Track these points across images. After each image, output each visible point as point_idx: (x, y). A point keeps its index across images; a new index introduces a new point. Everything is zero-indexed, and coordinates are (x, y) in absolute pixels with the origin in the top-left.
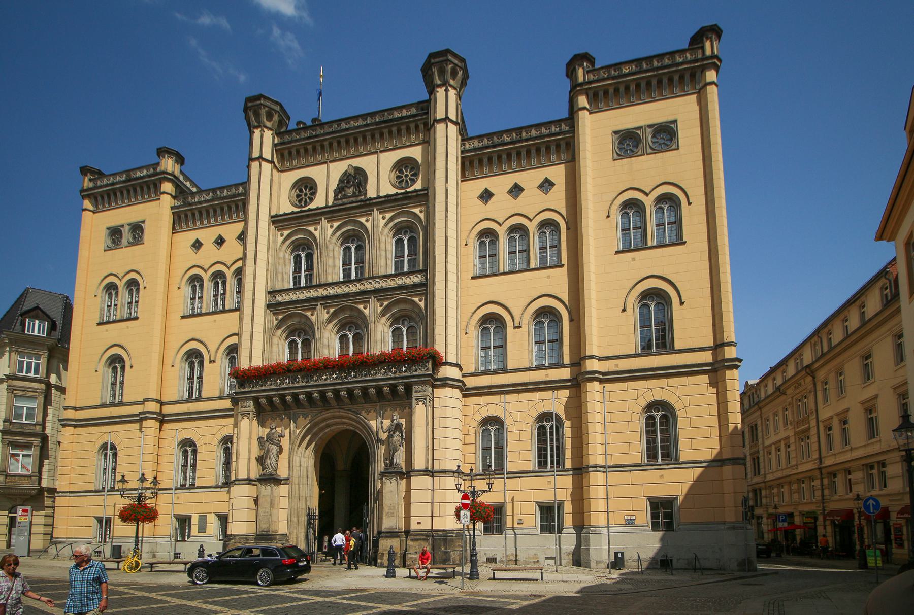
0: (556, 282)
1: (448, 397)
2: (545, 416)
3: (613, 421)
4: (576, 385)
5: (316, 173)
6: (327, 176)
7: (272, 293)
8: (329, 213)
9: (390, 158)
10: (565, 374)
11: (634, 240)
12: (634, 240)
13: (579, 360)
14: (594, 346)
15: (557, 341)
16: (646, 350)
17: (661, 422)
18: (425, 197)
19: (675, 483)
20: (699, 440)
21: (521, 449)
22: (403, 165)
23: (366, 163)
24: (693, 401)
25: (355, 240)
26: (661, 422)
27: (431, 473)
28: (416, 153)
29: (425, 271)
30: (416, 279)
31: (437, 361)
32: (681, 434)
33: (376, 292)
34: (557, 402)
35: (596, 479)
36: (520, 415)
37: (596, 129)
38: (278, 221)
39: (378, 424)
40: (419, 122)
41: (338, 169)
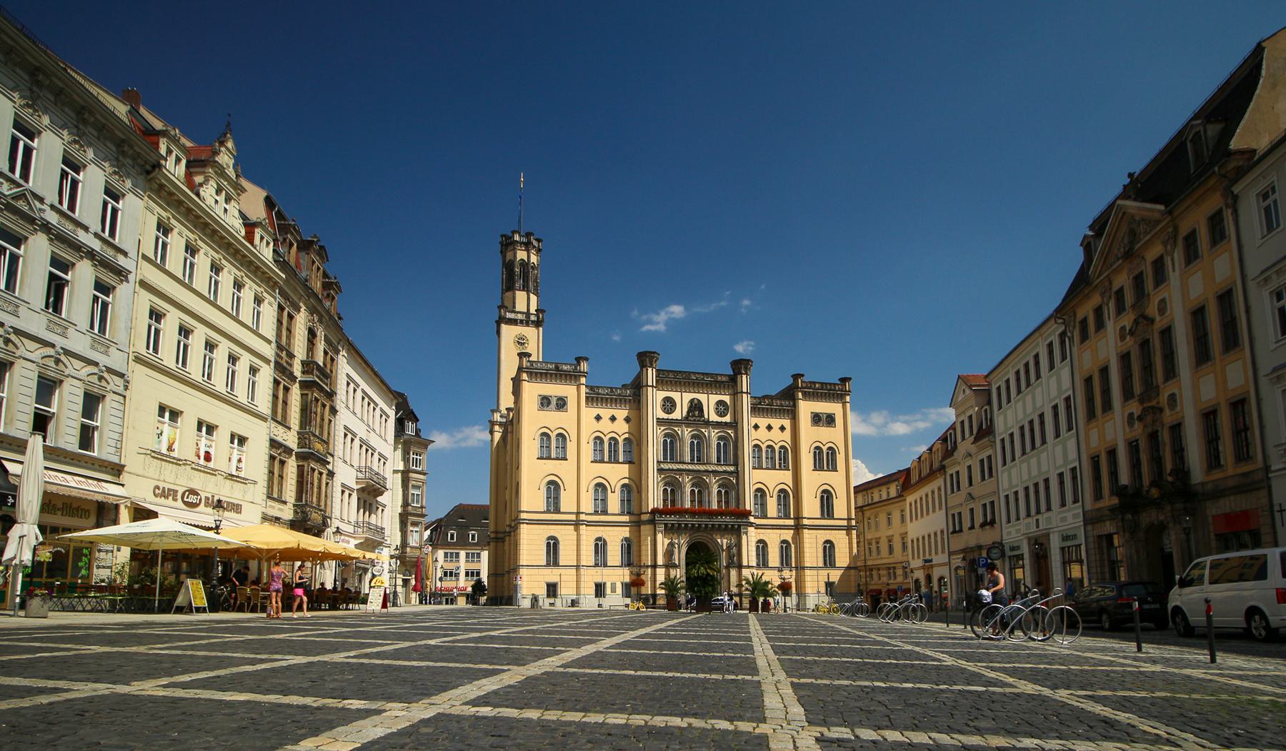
0: (786, 477)
1: (751, 529)
2: (784, 542)
3: (812, 544)
4: (798, 528)
5: (676, 396)
6: (683, 399)
7: (658, 462)
8: (685, 421)
9: (715, 398)
10: (791, 522)
11: (818, 466)
12: (818, 466)
13: (798, 518)
14: (806, 513)
15: (786, 506)
16: (823, 518)
17: (829, 548)
18: (735, 425)
19: (835, 576)
20: (842, 559)
21: (774, 558)
22: (720, 403)
23: (702, 397)
24: (841, 541)
25: (699, 443)
26: (829, 548)
27: (749, 567)
28: (727, 399)
29: (736, 464)
30: (732, 469)
31: (750, 512)
32: (837, 555)
33: (713, 472)
34: (788, 535)
35: (807, 572)
36: (774, 540)
37: (806, 408)
38: (660, 422)
39: (724, 542)
40: (731, 384)
41: (688, 397)
